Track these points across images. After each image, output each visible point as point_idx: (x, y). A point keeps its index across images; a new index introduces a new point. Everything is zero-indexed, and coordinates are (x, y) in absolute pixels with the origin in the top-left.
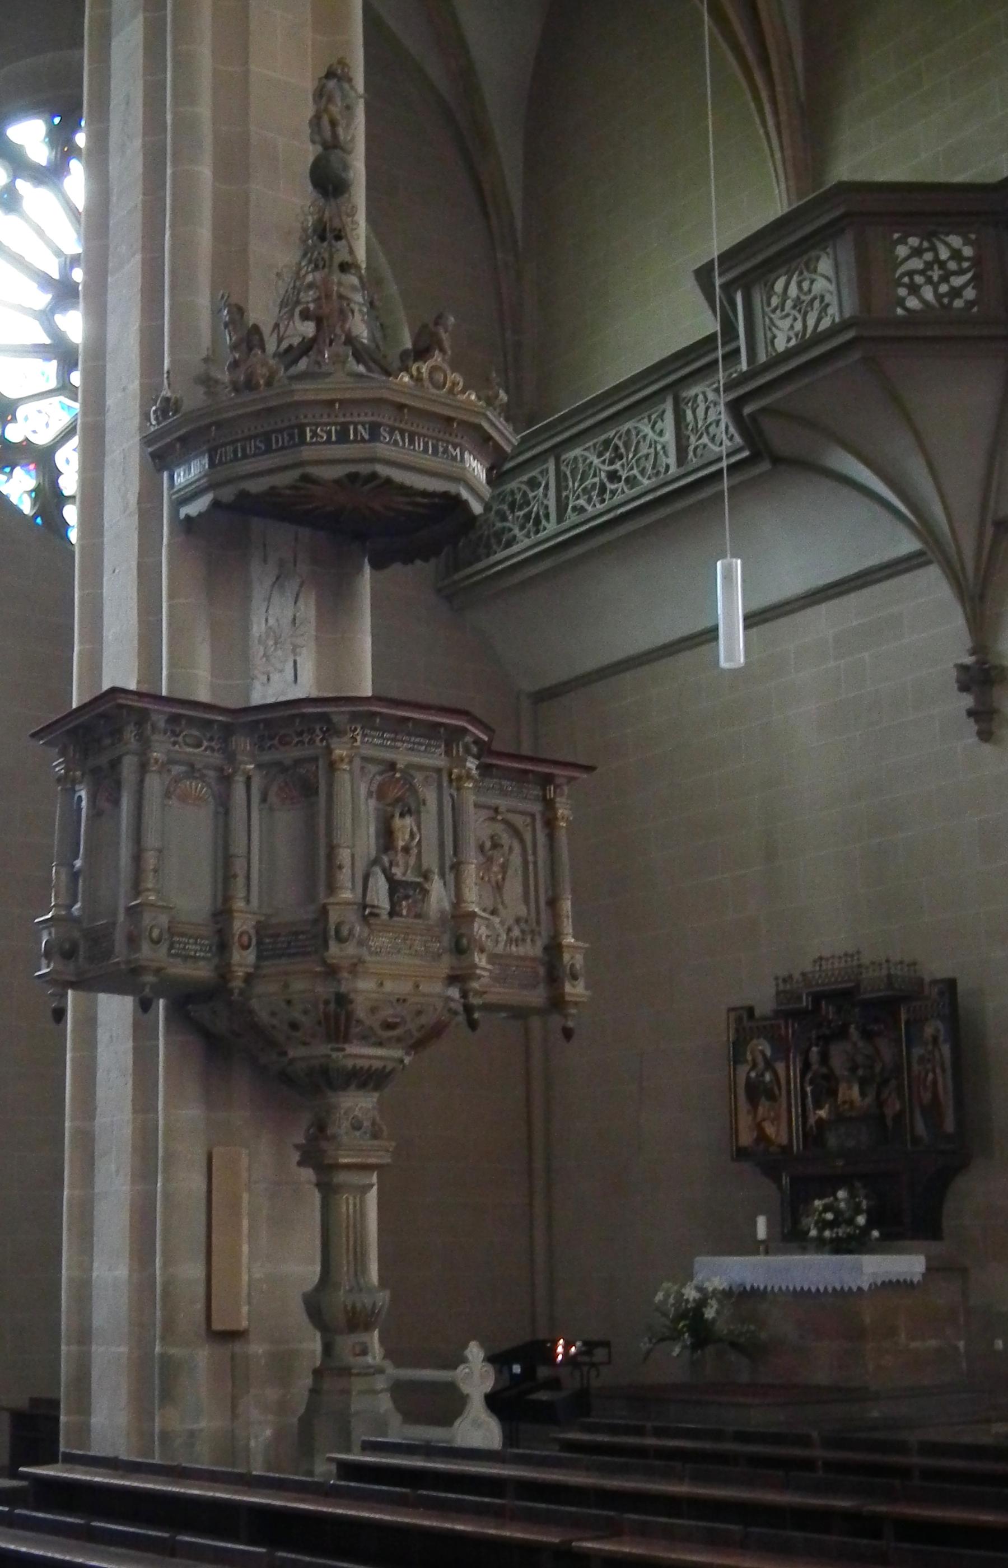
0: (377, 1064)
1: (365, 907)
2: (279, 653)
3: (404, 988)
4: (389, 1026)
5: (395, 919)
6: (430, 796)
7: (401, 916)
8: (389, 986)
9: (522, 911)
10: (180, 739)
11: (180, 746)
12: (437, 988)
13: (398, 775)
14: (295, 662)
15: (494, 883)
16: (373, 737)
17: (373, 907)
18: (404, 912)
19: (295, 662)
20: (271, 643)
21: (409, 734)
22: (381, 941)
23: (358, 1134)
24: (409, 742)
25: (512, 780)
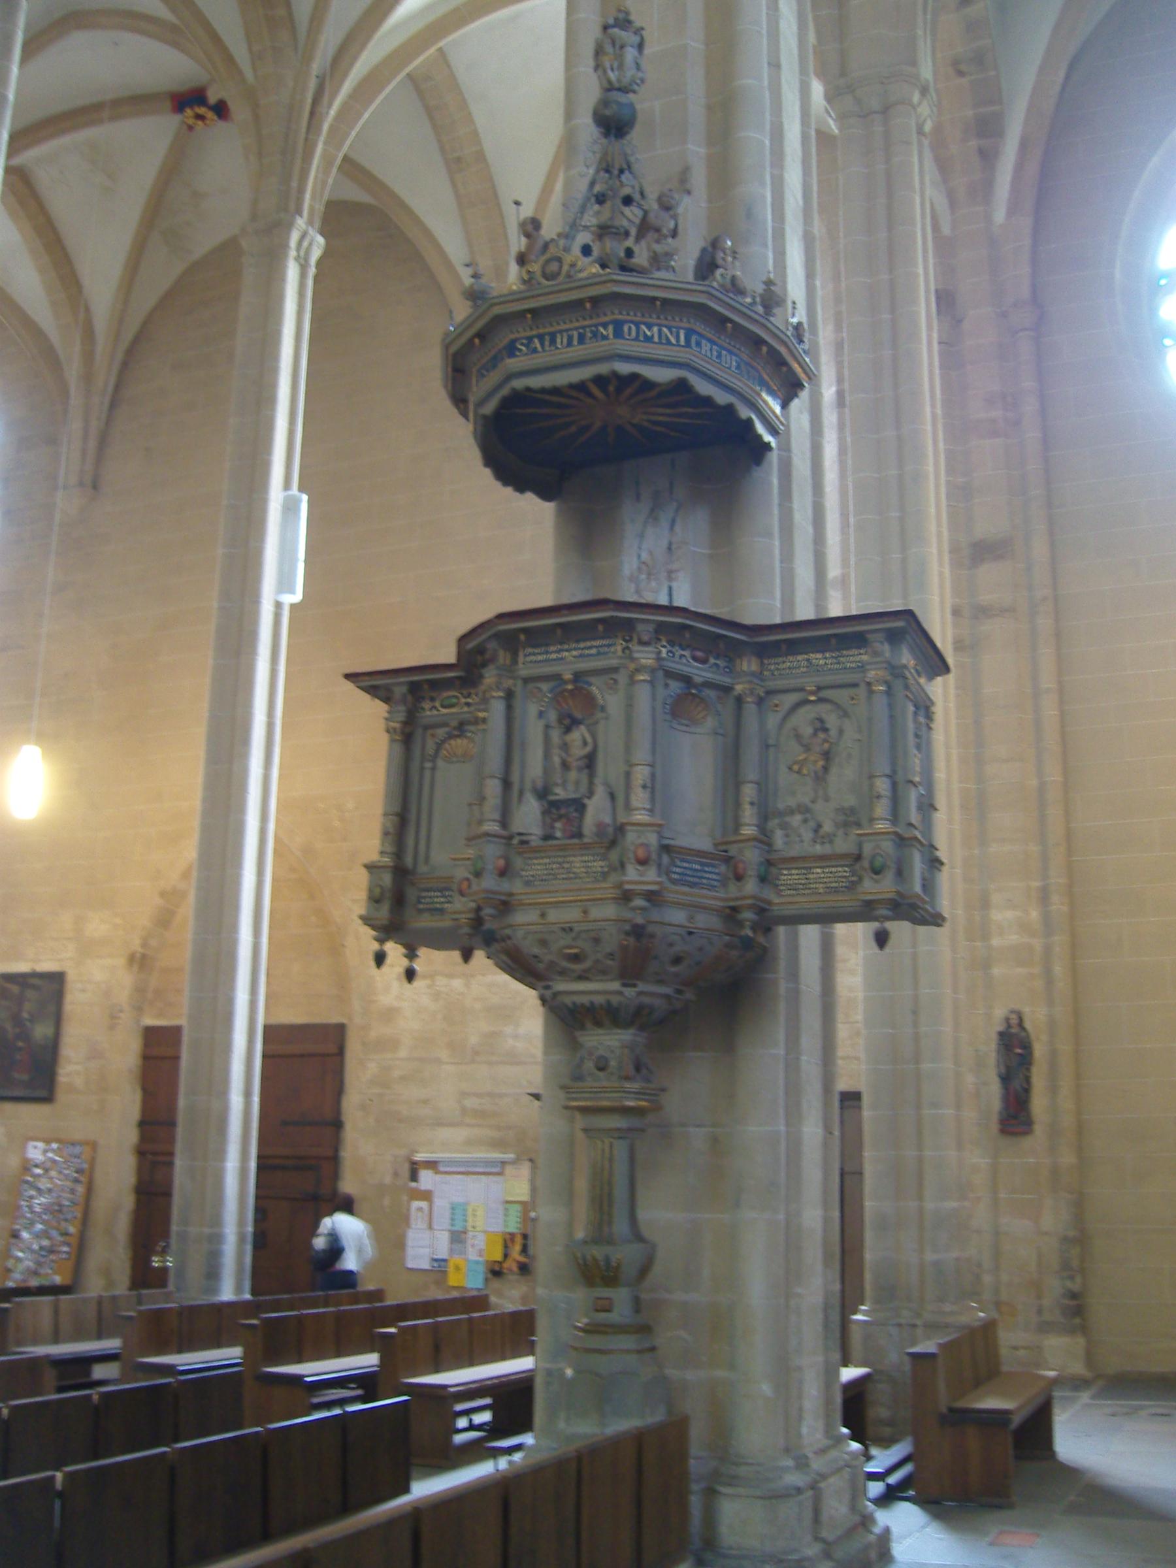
0: (599, 1000)
1: (511, 838)
2: (653, 584)
3: (571, 915)
4: (576, 958)
5: (550, 842)
6: (613, 703)
7: (556, 839)
8: (553, 916)
9: (850, 801)
10: (437, 704)
11: (438, 710)
12: (609, 911)
13: (570, 687)
14: (670, 589)
15: (813, 774)
16: (534, 654)
17: (520, 834)
18: (558, 834)
19: (670, 589)
20: (643, 576)
21: (578, 641)
22: (537, 867)
23: (601, 1074)
24: (575, 649)
25: (823, 652)
